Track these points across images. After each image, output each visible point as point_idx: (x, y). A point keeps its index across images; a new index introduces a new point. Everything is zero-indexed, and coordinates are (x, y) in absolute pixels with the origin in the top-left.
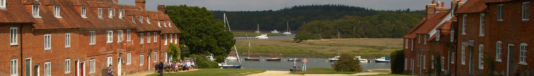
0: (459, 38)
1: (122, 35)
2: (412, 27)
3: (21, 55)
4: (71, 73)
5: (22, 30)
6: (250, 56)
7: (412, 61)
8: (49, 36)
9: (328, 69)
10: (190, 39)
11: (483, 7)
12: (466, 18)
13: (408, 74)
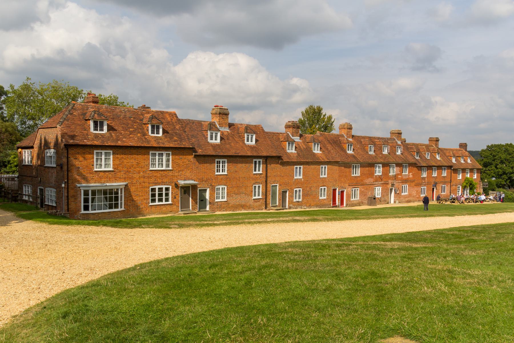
3: (266, 181)
4: (327, 199)
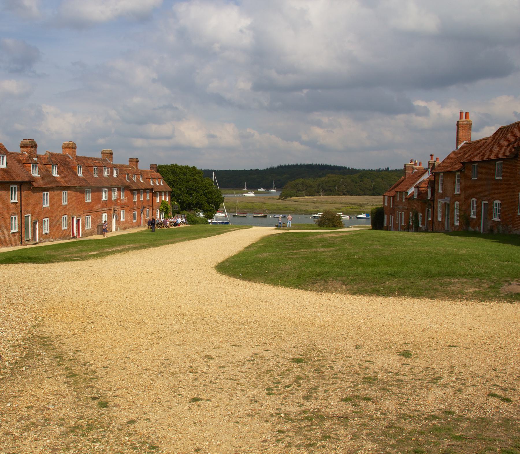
0: (436, 196)
1: (117, 193)
2: (391, 185)
3: (21, 211)
4: (68, 229)
6: (238, 213)
7: (392, 218)
8: (47, 194)
9: (312, 225)
10: (181, 197)
11: (458, 166)
12: (443, 176)
13: (387, 230)
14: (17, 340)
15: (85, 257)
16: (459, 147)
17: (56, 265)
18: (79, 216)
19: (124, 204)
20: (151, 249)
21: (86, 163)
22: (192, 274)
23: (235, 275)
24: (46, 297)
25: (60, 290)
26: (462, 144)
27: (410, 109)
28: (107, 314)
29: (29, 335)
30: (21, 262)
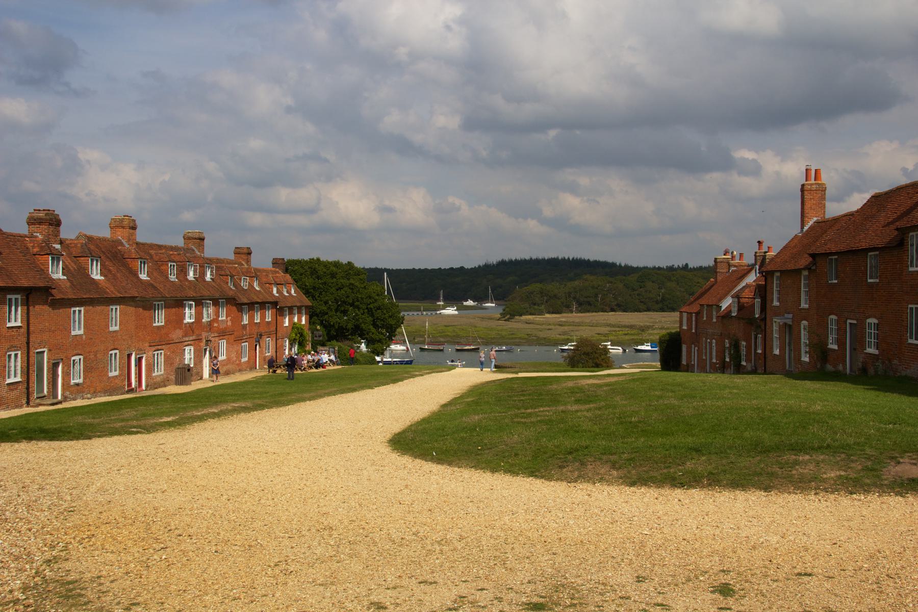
0: (768, 311)
1: (211, 310)
2: (692, 294)
3: (28, 343)
4: (120, 375)
5: (31, 300)
6: (428, 344)
7: (694, 349)
8: (80, 311)
9: (558, 365)
10: (326, 317)
11: (805, 261)
12: (779, 278)
13: (687, 371)
14: (11, 591)
15: (151, 427)
16: (806, 228)
17: (96, 442)
18: (140, 351)
19: (226, 328)
20: (274, 409)
21: (155, 254)
22: (347, 455)
23: (424, 455)
24: (74, 505)
25: (102, 490)
26: (811, 223)
27: (726, 164)
28: (191, 531)
29: (37, 579)
30: (25, 438)
